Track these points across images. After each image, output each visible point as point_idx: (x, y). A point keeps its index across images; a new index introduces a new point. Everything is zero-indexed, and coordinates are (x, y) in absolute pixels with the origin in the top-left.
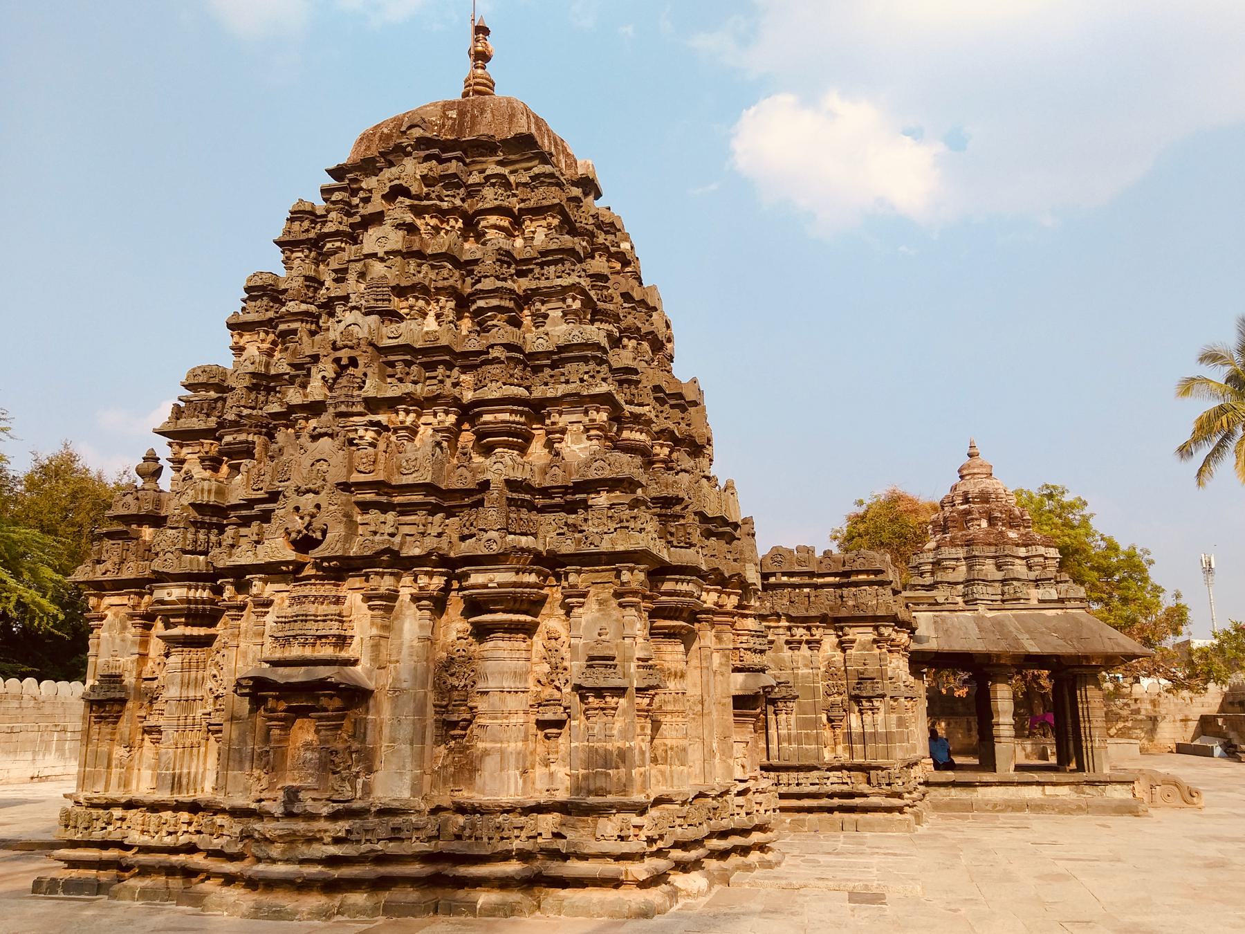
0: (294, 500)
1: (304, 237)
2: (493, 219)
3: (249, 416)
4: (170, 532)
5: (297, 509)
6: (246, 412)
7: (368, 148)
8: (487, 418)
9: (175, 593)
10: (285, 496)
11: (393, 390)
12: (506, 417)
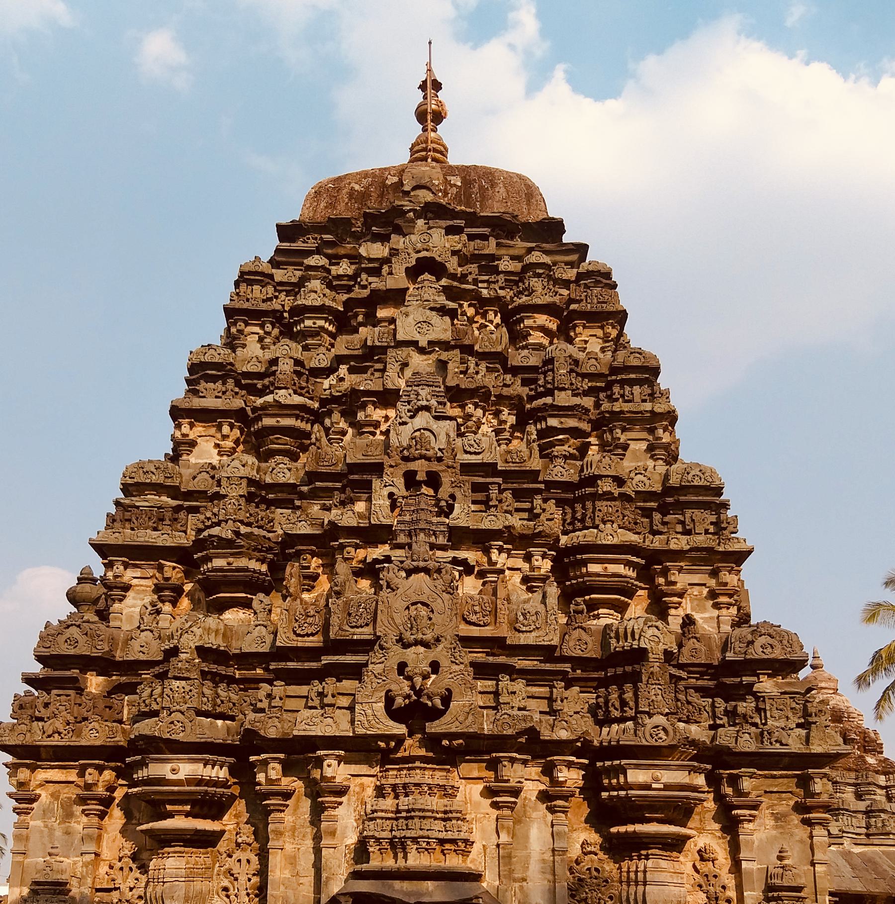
0: (397, 654)
1: (264, 307)
2: (542, 319)
3: (248, 536)
4: (176, 684)
5: (402, 667)
6: (243, 530)
7: (331, 206)
8: (594, 568)
9: (185, 769)
10: (382, 648)
11: (490, 522)
12: (620, 569)
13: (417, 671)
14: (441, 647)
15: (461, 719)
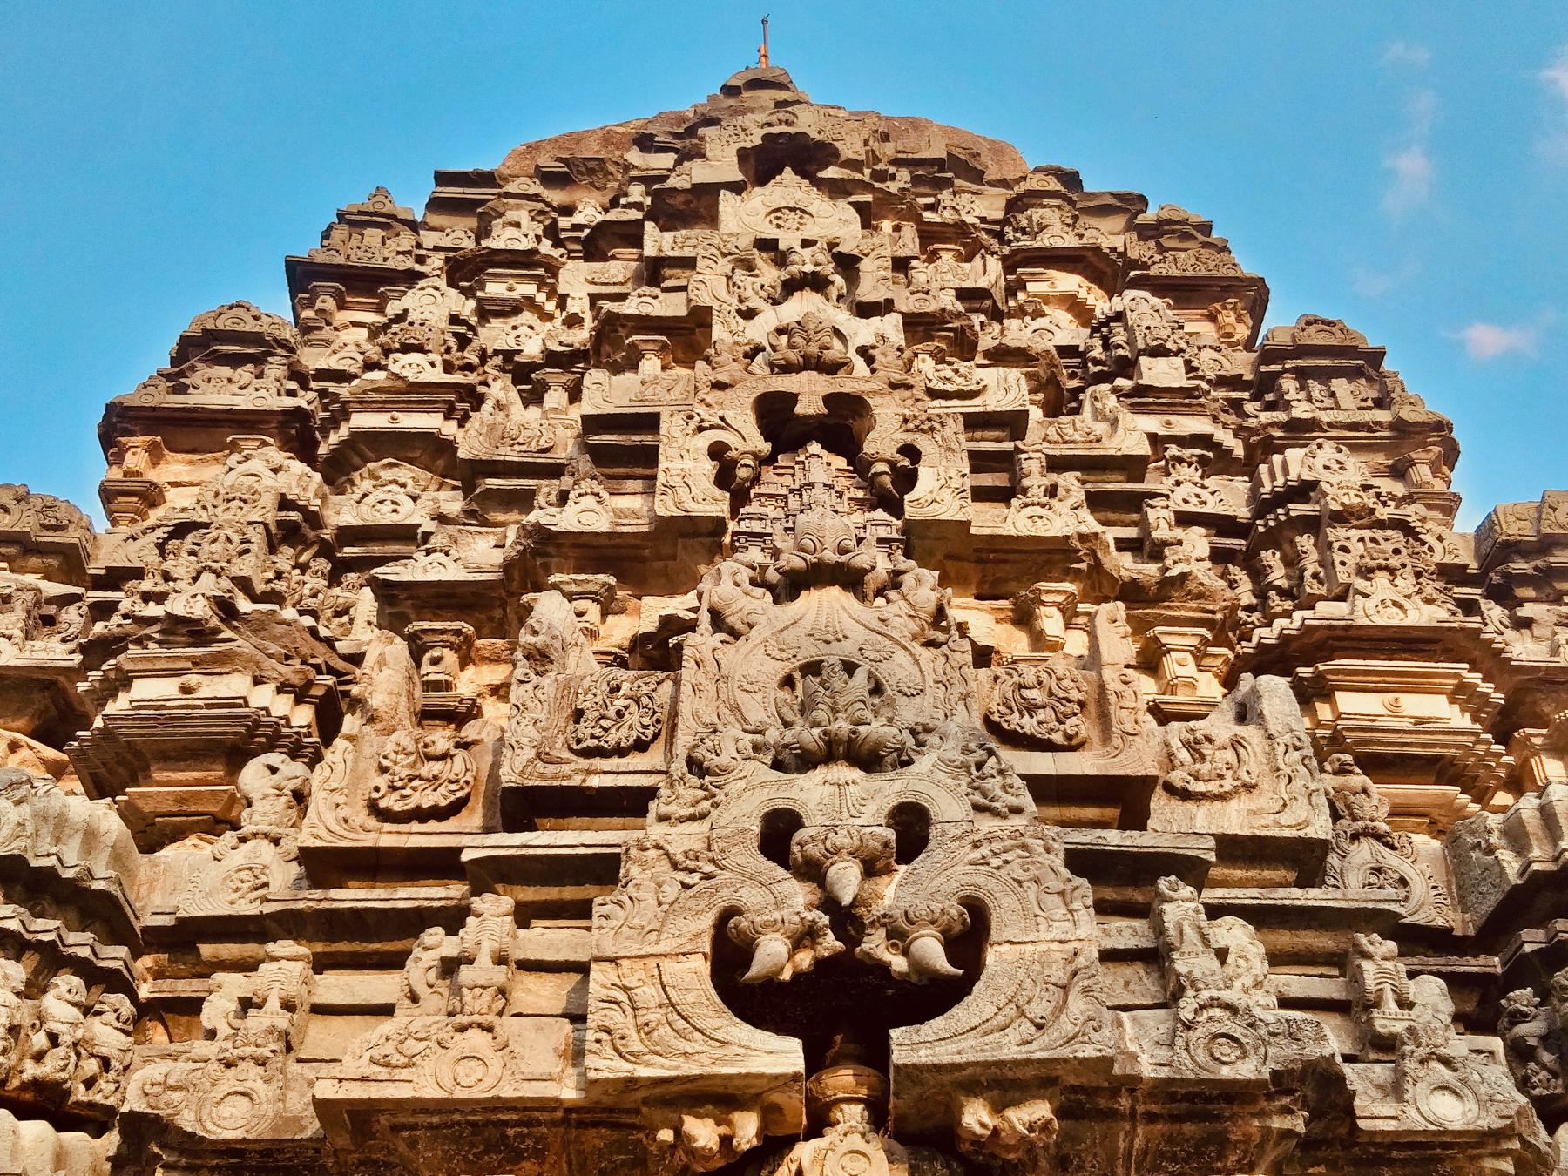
5: (778, 835)
13: (841, 839)
14: (923, 764)
15: (1037, 1009)
